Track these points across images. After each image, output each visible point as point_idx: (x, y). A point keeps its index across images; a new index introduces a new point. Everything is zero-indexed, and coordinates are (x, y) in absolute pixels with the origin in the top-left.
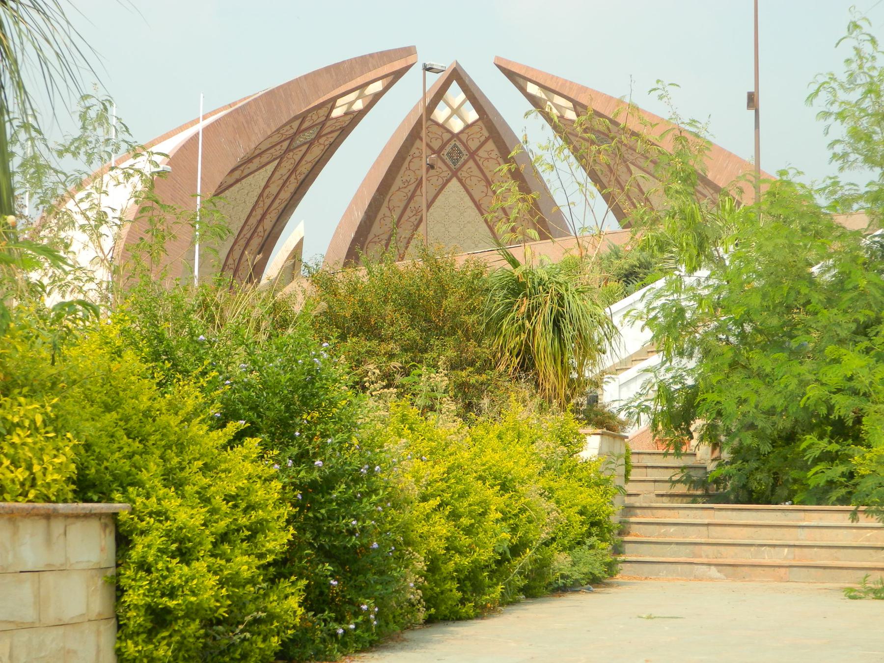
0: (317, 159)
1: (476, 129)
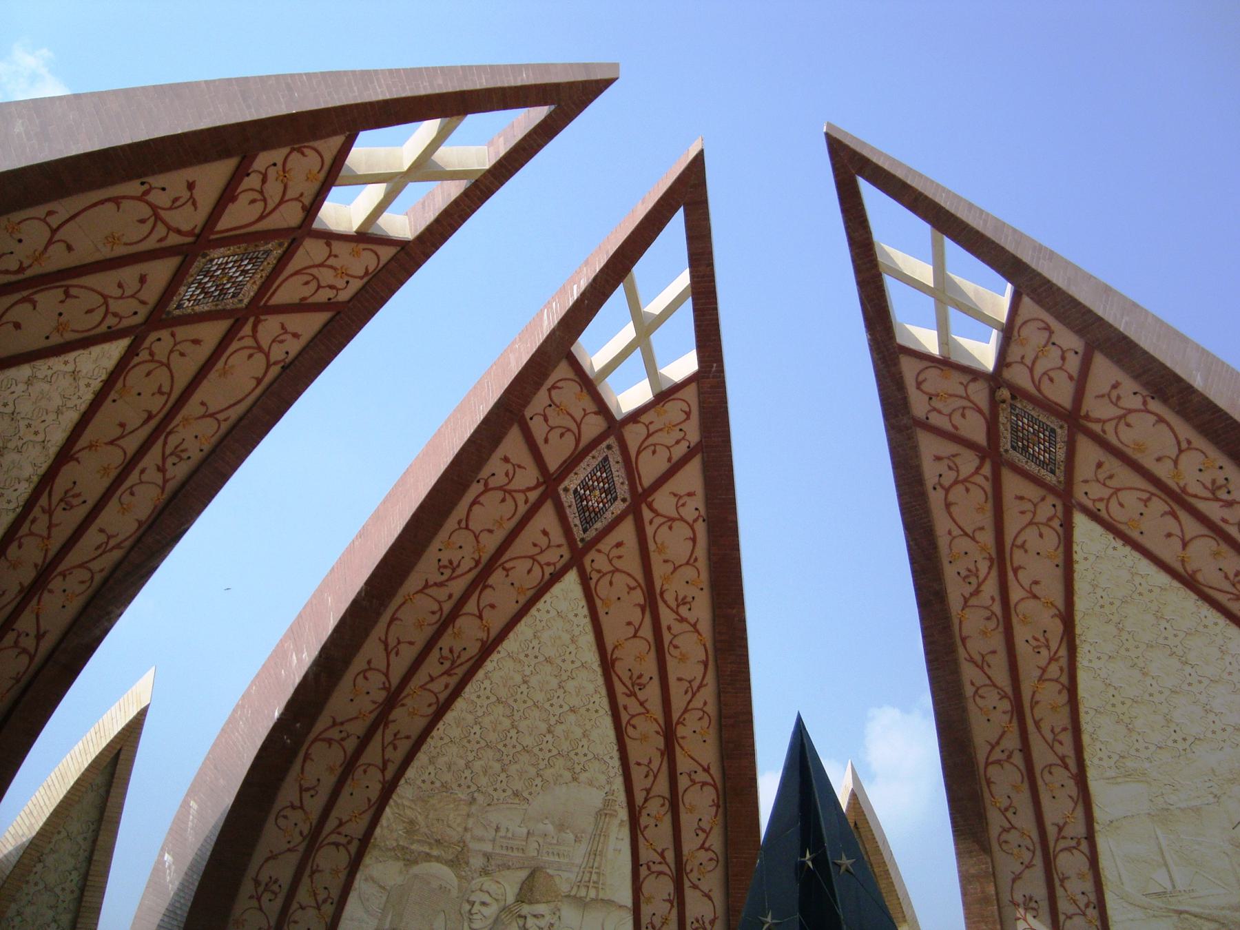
0: (235, 413)
1: (673, 410)
